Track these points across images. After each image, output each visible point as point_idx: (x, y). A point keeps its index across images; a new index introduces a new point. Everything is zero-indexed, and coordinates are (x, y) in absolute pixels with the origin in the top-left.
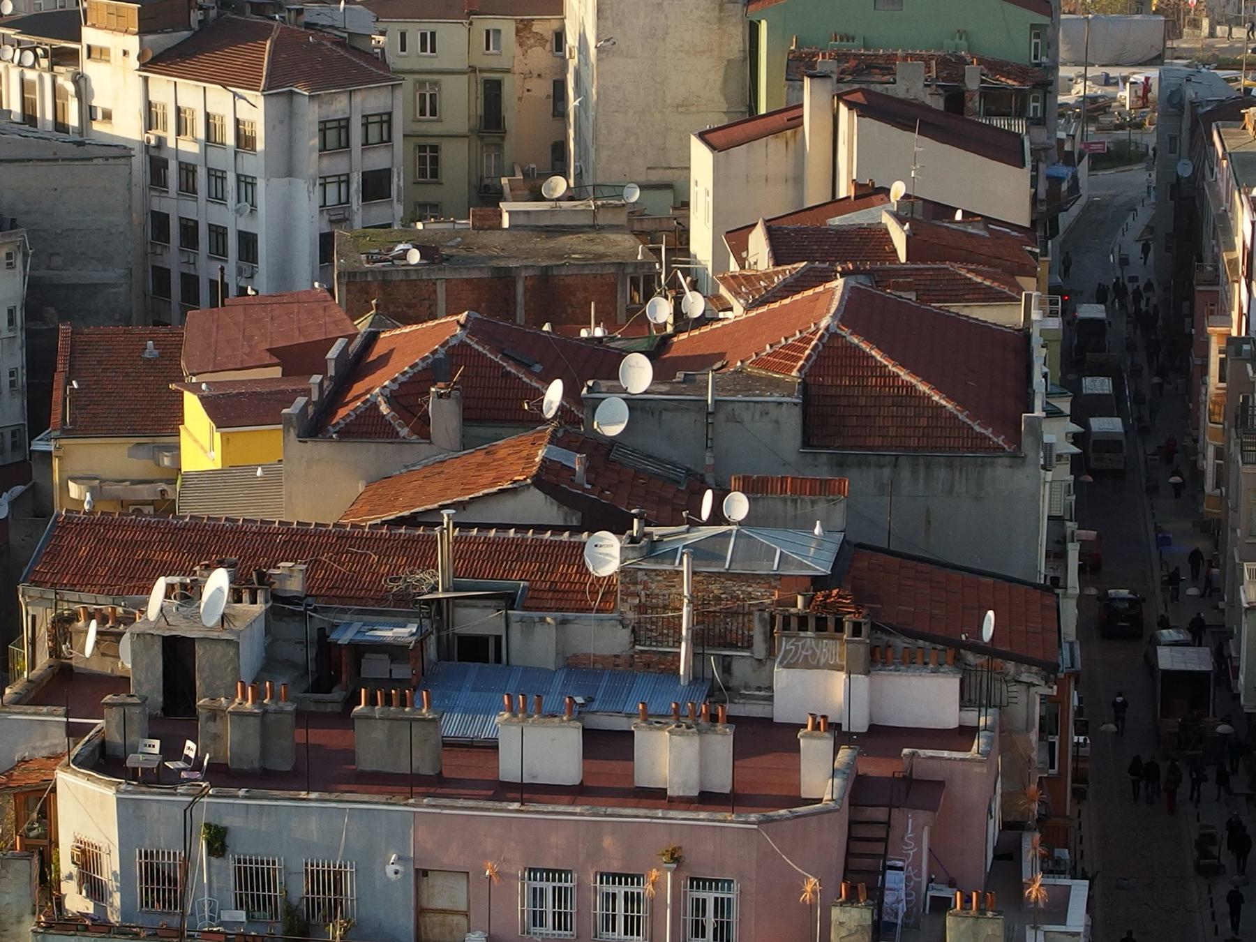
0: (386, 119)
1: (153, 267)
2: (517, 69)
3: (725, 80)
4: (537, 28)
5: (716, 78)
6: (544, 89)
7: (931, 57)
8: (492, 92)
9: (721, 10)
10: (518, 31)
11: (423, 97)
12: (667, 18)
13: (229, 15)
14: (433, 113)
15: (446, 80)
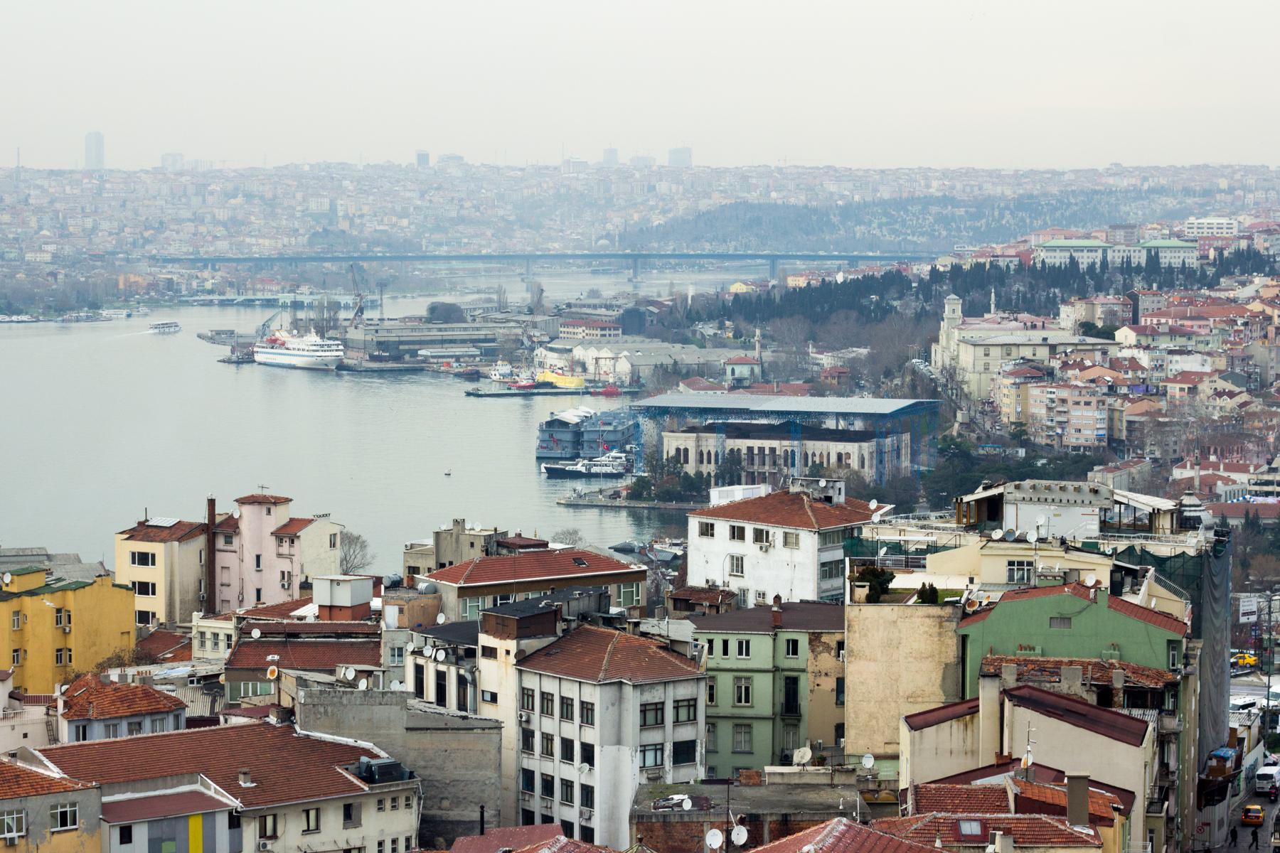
0: (692, 703)
1: (523, 810)
2: (810, 669)
3: (944, 679)
4: (825, 639)
5: (937, 677)
6: (829, 684)
7: (1089, 663)
8: (791, 686)
9: (941, 626)
10: (811, 642)
11: (739, 688)
12: (900, 632)
13: (587, 626)
14: (747, 701)
15: (757, 677)
